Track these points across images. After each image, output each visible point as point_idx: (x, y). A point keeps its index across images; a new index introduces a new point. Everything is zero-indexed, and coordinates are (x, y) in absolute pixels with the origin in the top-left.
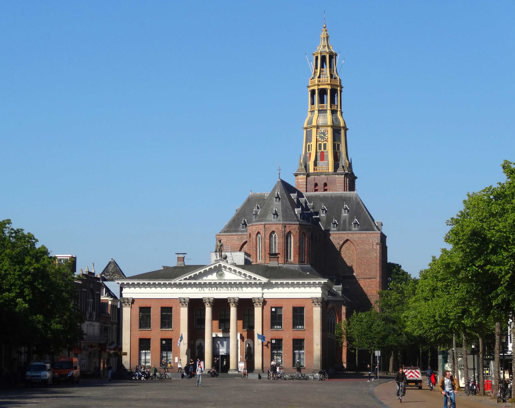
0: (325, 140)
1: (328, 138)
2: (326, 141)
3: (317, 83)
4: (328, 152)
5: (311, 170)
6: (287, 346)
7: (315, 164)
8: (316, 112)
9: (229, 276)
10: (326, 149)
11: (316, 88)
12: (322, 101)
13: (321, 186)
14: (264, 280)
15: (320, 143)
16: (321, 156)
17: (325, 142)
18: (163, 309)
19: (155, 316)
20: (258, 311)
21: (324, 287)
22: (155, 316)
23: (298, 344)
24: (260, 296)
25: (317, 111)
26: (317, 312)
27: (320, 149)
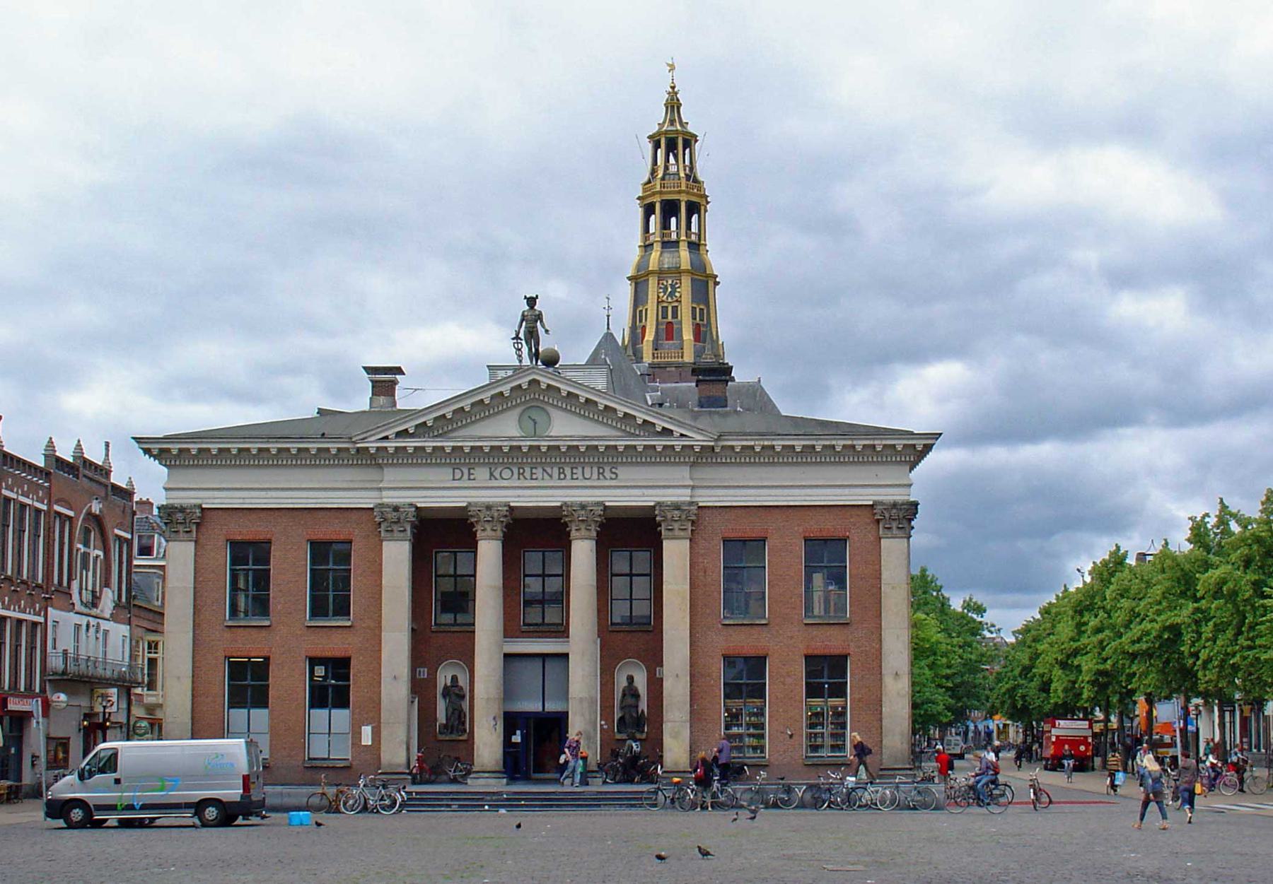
0: (675, 299)
1: (681, 296)
2: (677, 301)
3: (658, 188)
4: (681, 323)
7: (656, 347)
8: (657, 247)
10: (677, 318)
11: (657, 199)
12: (665, 225)
15: (665, 305)
16: (669, 331)
17: (676, 304)
25: (660, 244)
27: (665, 316)
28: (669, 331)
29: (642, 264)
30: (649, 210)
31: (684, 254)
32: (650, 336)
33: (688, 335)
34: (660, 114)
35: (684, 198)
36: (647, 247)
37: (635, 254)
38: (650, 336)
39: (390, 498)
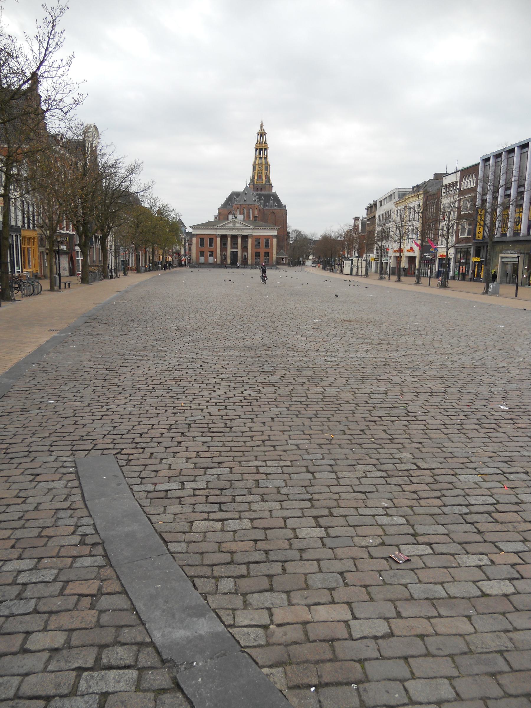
5: (255, 183)
6: (262, 255)
8: (258, 159)
9: (238, 225)
12: (260, 154)
13: (259, 189)
14: (253, 227)
16: (260, 177)
18: (210, 239)
19: (207, 241)
20: (250, 240)
21: (278, 230)
22: (207, 241)
23: (267, 254)
24: (251, 234)
26: (275, 241)
28: (260, 177)
29: (255, 162)
30: (256, 150)
31: (263, 160)
32: (256, 178)
33: (264, 178)
34: (259, 128)
35: (263, 148)
36: (256, 158)
37: (253, 159)
38: (256, 178)
39: (218, 233)
